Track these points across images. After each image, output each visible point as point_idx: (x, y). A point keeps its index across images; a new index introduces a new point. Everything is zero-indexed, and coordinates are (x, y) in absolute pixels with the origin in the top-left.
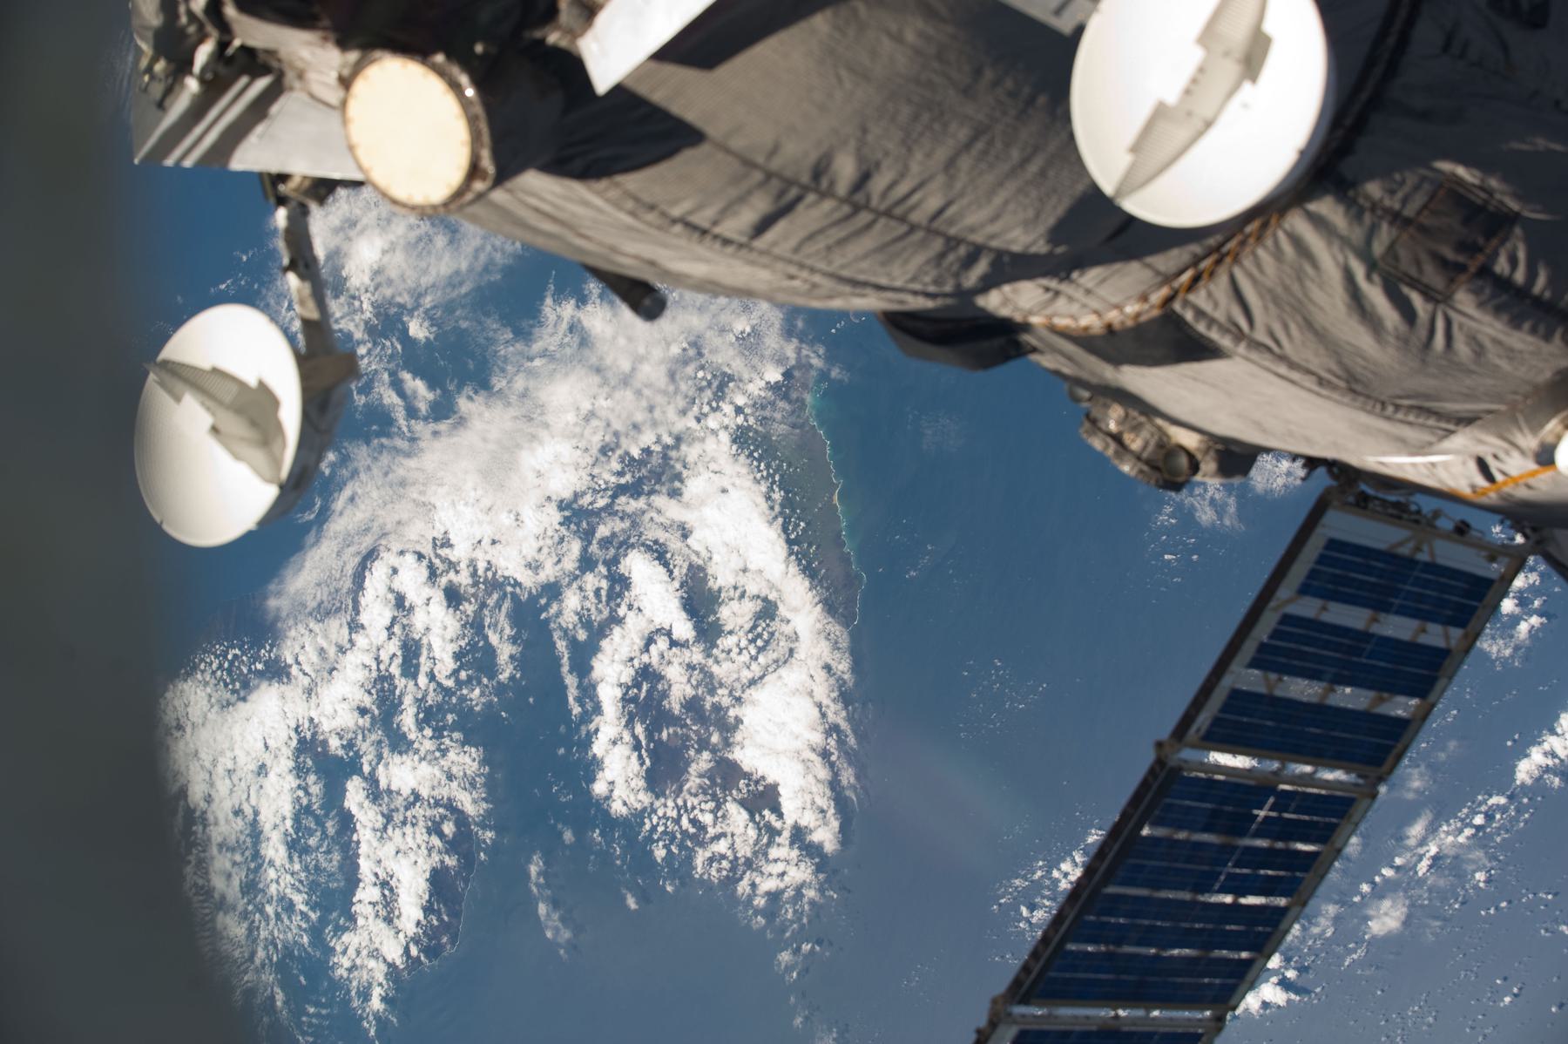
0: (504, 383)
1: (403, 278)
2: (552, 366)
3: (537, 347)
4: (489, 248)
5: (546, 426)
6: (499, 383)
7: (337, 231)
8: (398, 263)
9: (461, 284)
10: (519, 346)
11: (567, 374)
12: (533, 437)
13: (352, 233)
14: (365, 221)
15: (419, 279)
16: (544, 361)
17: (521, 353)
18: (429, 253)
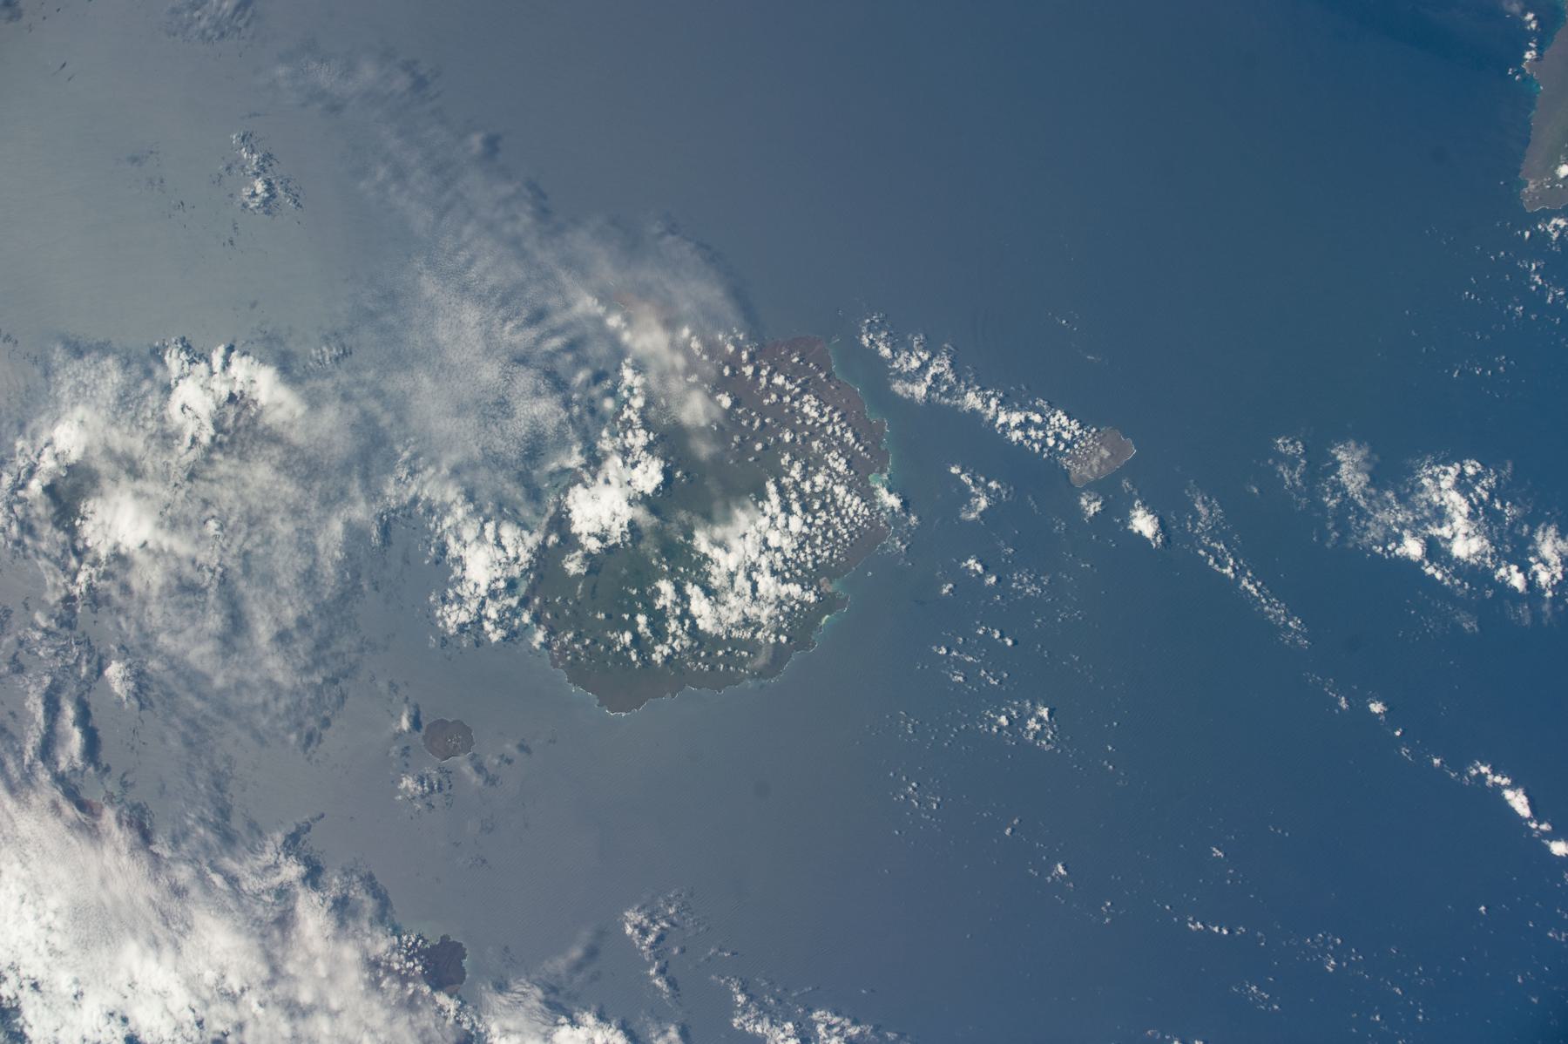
0: (166, 853)
1: (144, 602)
2: (230, 903)
3: (228, 863)
4: (259, 700)
5: (178, 949)
6: (162, 848)
7: (109, 452)
8: (150, 577)
9: (201, 696)
10: (212, 838)
11: (238, 930)
12: (155, 944)
13: (124, 480)
14: (149, 487)
15: (160, 630)
16: (226, 887)
17: (205, 845)
18: (193, 619)
